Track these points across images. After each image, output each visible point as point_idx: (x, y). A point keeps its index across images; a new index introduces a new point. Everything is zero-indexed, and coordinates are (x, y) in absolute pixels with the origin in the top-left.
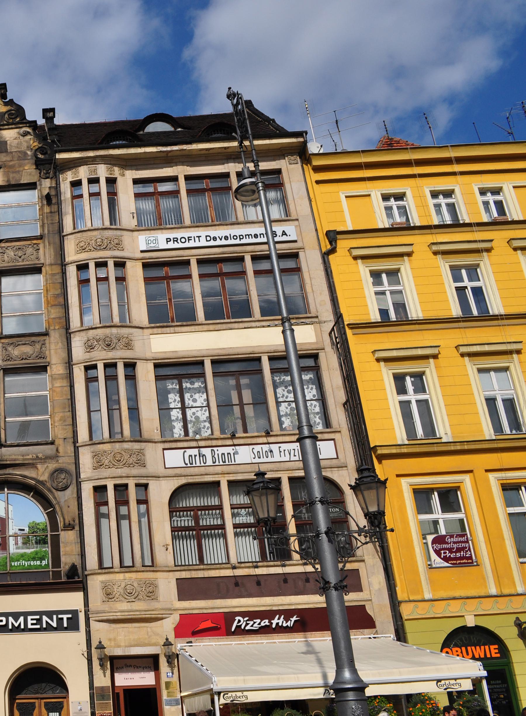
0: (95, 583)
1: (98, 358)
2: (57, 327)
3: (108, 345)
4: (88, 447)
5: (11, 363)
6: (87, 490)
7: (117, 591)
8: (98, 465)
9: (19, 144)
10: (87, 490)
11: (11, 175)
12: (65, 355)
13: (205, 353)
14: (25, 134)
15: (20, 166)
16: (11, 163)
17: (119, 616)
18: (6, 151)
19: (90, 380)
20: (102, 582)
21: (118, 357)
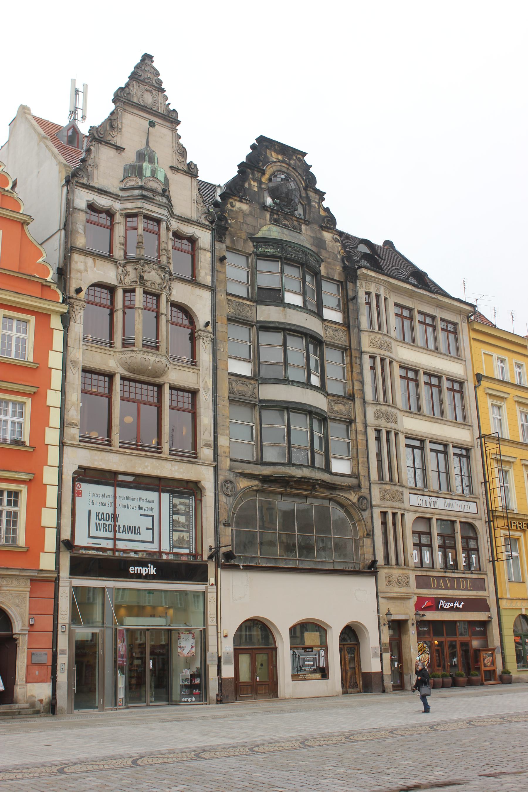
0: (383, 573)
1: (384, 426)
2: (359, 397)
3: (388, 418)
4: (378, 485)
5: (336, 415)
6: (377, 513)
7: (394, 579)
8: (383, 498)
9: (333, 246)
10: (377, 513)
11: (330, 270)
12: (363, 418)
13: (426, 435)
14: (336, 241)
15: (334, 265)
16: (329, 260)
17: (395, 595)
18: (326, 249)
19: (378, 439)
20: (386, 574)
21: (393, 428)
